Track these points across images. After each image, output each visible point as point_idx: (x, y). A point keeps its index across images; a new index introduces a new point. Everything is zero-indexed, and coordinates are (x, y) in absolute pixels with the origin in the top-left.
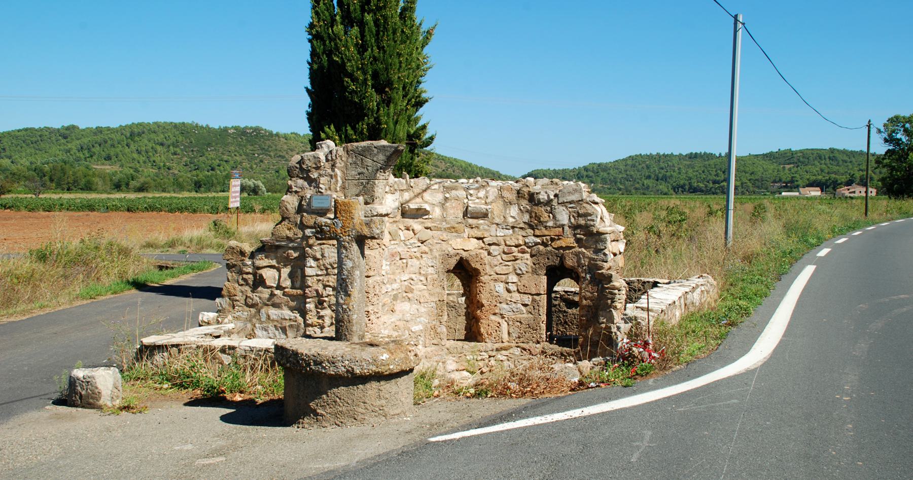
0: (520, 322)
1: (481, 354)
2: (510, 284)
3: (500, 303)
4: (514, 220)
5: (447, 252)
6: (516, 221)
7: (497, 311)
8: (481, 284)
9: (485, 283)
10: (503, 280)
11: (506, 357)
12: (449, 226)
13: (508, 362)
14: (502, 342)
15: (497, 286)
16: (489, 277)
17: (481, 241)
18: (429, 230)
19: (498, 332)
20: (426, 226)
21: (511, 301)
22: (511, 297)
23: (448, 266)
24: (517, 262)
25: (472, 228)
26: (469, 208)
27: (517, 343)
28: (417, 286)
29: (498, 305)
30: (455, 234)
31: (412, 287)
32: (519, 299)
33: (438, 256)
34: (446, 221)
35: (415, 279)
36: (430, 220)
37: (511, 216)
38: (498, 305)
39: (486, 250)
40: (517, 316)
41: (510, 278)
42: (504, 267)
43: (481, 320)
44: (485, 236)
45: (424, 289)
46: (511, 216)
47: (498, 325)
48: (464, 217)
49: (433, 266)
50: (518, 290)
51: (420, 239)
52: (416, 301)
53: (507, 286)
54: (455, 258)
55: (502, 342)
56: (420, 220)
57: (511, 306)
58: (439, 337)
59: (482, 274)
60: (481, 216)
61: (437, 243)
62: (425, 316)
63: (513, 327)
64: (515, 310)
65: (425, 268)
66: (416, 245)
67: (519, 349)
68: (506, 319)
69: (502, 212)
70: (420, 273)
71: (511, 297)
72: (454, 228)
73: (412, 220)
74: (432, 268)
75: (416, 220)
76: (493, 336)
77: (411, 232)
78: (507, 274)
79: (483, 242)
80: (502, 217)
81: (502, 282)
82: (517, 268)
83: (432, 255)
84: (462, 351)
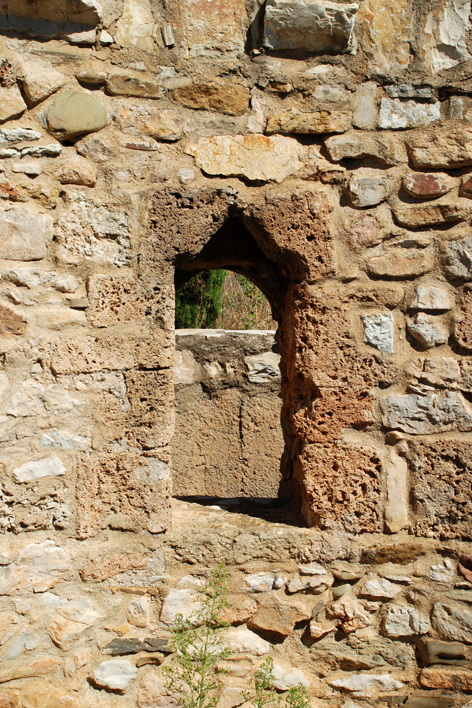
0: (458, 462)
1: (305, 568)
2: (421, 316)
3: (383, 385)
4: (450, 63)
5: (173, 184)
6: (462, 65)
7: (368, 416)
8: (310, 311)
9: (324, 310)
10: (397, 299)
11: (398, 589)
12: (186, 82)
13: (407, 607)
14: (387, 531)
15: (369, 322)
16: (342, 288)
17: (315, 149)
18: (100, 93)
19: (372, 494)
20: (83, 72)
21: (423, 381)
22: (425, 366)
23: (178, 240)
24: (455, 231)
25: (283, 95)
26: (269, 8)
27: (442, 538)
28: (43, 310)
29: (373, 391)
30: (215, 117)
31: (17, 311)
32: (456, 375)
33: (135, 199)
34: (174, 61)
35: (34, 282)
36: (104, 53)
37: (442, 48)
38: (373, 391)
39: (334, 182)
40: (447, 438)
41: (423, 291)
42: (402, 252)
43: (308, 448)
44: (333, 127)
45: (73, 323)
46: (442, 48)
47: (373, 468)
48: (248, 49)
49: (113, 237)
50: (452, 341)
51: (55, 124)
52: (37, 368)
53: (410, 322)
54: (207, 208)
55: (387, 531)
56: (53, 45)
57: (422, 401)
58: (137, 501)
59: (315, 275)
60: (319, 46)
61: (129, 146)
62: (76, 423)
63: (431, 478)
64: (439, 415)
65: (80, 241)
66: (36, 147)
67: (448, 561)
68: (404, 446)
69: (405, 31)
70: (56, 260)
71: (425, 366)
72: (207, 91)
73: (15, 41)
74: (112, 245)
75: (36, 45)
76: (353, 506)
77: (15, 91)
78: (412, 277)
79: (325, 152)
80: (404, 53)
81: (391, 307)
82: (452, 254)
83: (109, 191)
84: (230, 556)
